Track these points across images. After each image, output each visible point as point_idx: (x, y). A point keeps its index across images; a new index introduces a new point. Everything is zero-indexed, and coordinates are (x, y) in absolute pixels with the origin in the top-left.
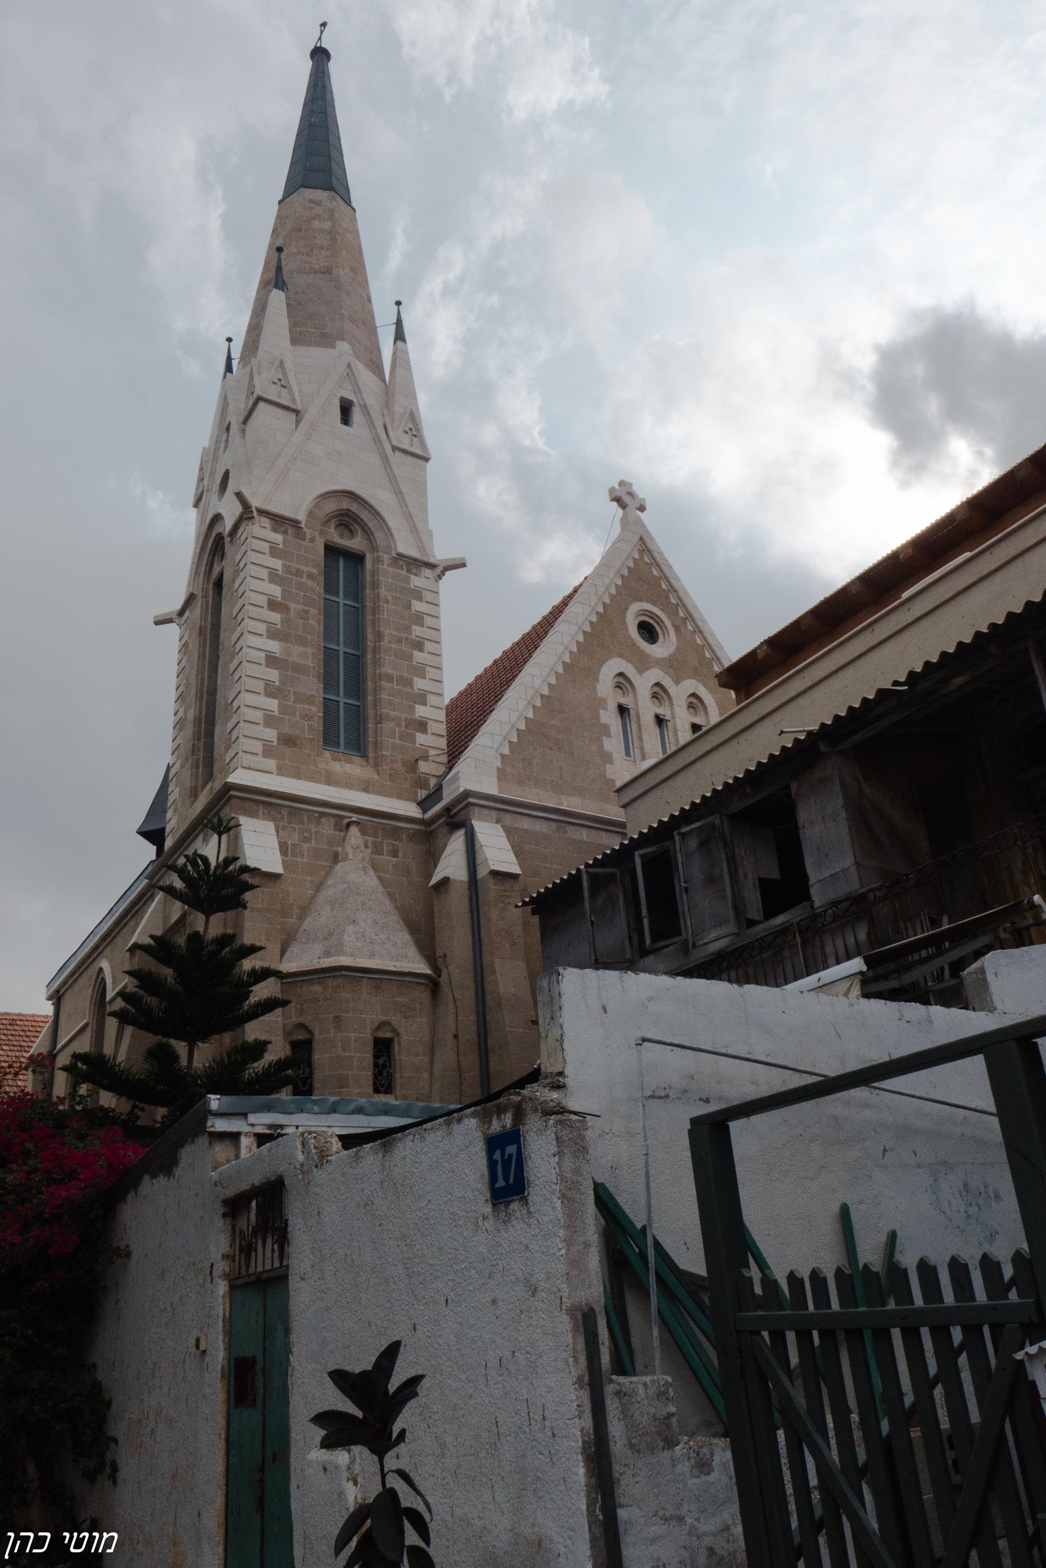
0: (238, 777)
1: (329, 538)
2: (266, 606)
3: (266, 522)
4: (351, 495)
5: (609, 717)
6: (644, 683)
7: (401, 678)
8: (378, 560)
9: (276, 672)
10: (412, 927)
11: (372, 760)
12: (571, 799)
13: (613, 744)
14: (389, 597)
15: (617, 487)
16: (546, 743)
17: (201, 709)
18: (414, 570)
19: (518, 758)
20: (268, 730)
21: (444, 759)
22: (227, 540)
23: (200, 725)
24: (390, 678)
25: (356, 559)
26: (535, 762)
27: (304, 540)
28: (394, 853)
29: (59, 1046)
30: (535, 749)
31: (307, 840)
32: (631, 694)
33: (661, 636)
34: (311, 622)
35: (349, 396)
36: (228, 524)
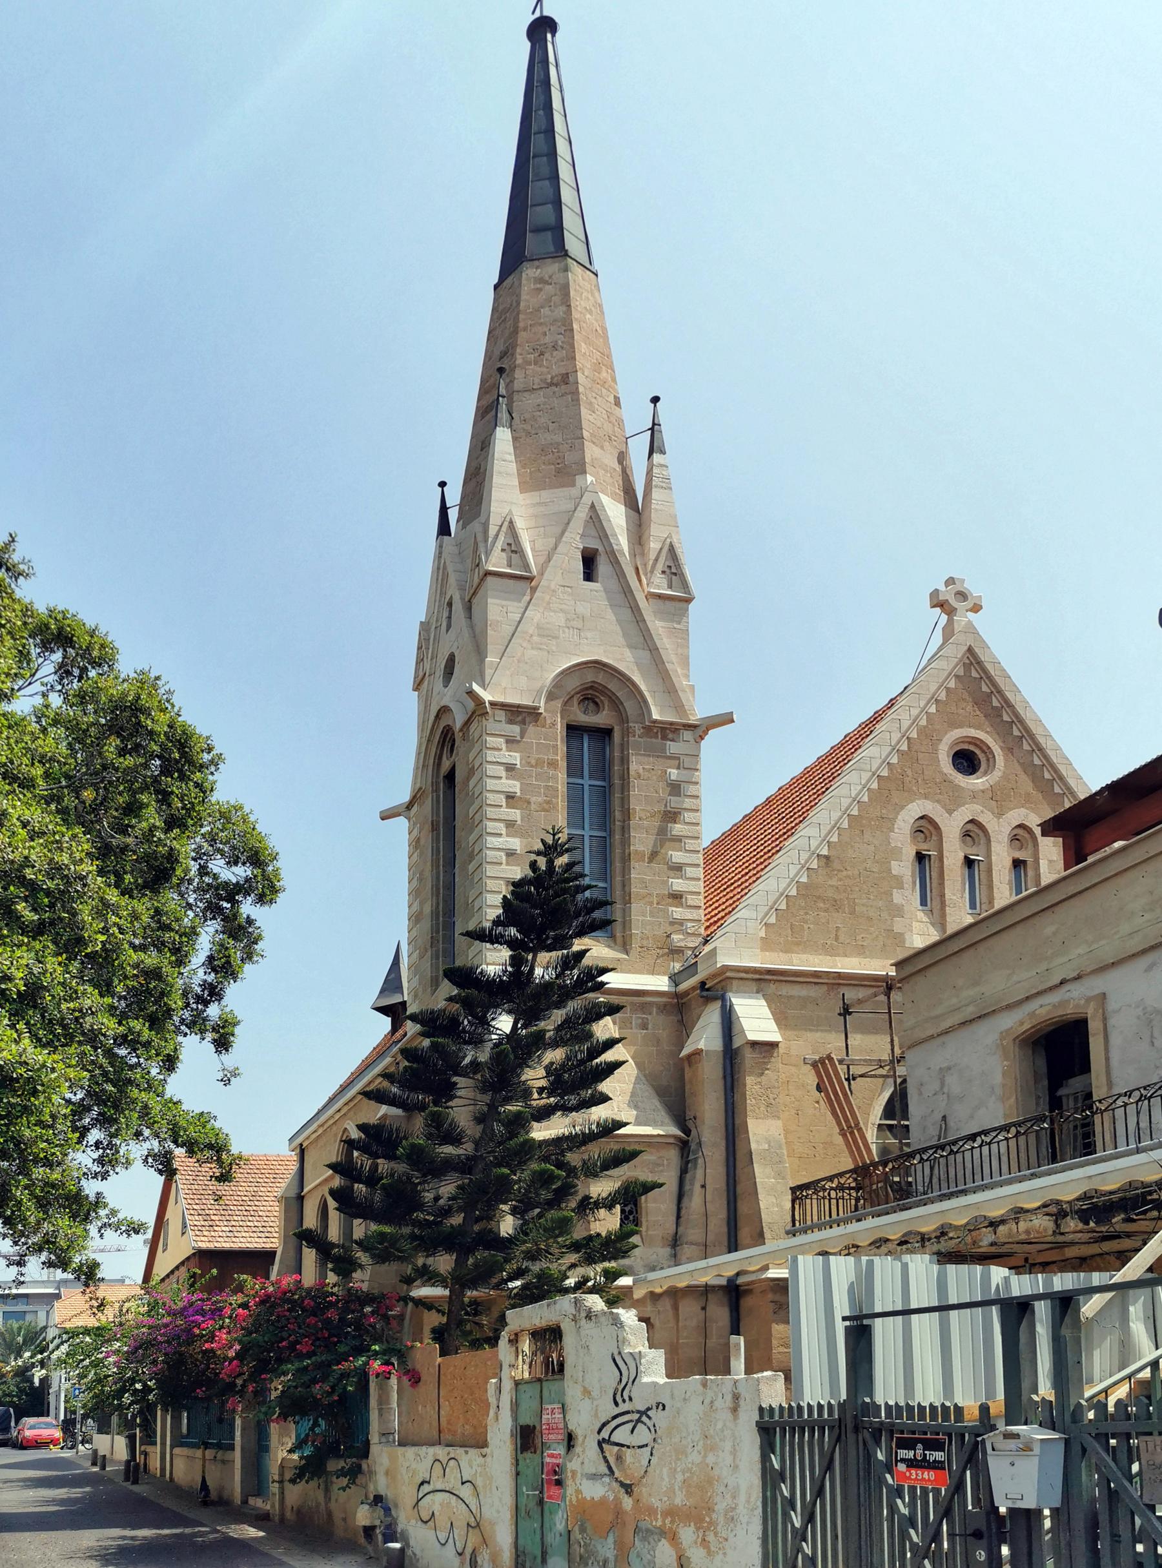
1: (572, 717)
5: (905, 867)
6: (952, 826)
8: (626, 733)
10: (661, 1093)
11: (619, 939)
12: (847, 960)
13: (908, 897)
14: (641, 771)
15: (942, 588)
16: (822, 905)
17: (438, 904)
18: (670, 736)
19: (787, 925)
22: (458, 736)
25: (603, 734)
28: (644, 1026)
30: (806, 914)
32: (934, 838)
33: (982, 769)
36: (459, 721)
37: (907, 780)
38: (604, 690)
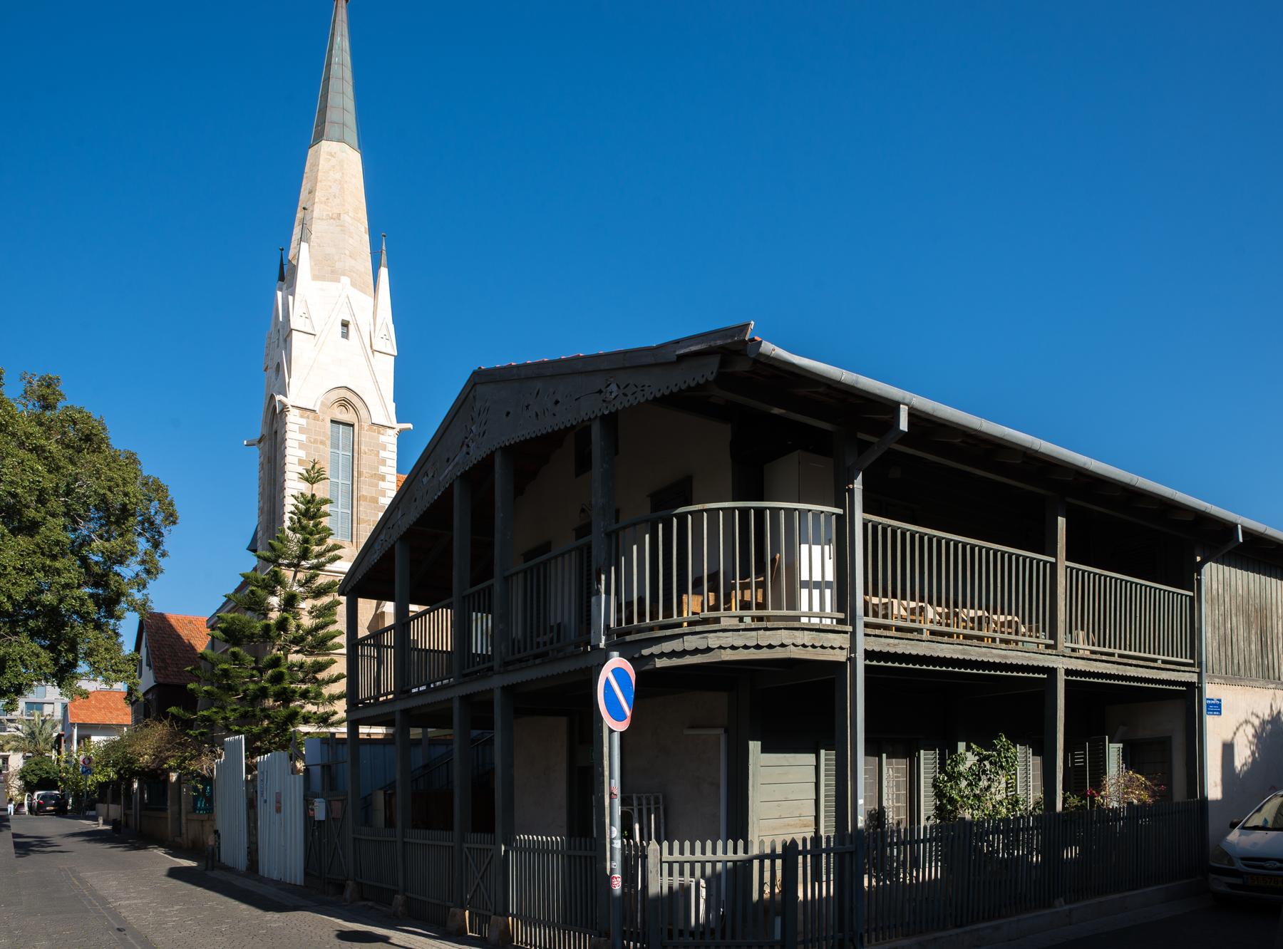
3: (297, 412)
35: (347, 318)
38: (350, 403)
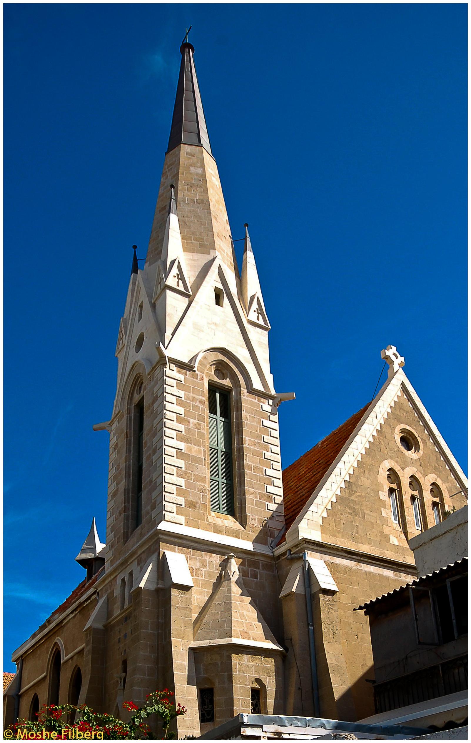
0: (163, 526)
2: (175, 420)
3: (173, 366)
4: (223, 351)
7: (256, 467)
9: (183, 462)
14: (248, 417)
16: (349, 511)
20: (179, 498)
21: (283, 519)
23: (128, 494)
24: (250, 468)
26: (342, 522)
27: (197, 379)
29: (22, 691)
30: (342, 514)
31: (204, 566)
34: (202, 431)
37: (382, 446)
